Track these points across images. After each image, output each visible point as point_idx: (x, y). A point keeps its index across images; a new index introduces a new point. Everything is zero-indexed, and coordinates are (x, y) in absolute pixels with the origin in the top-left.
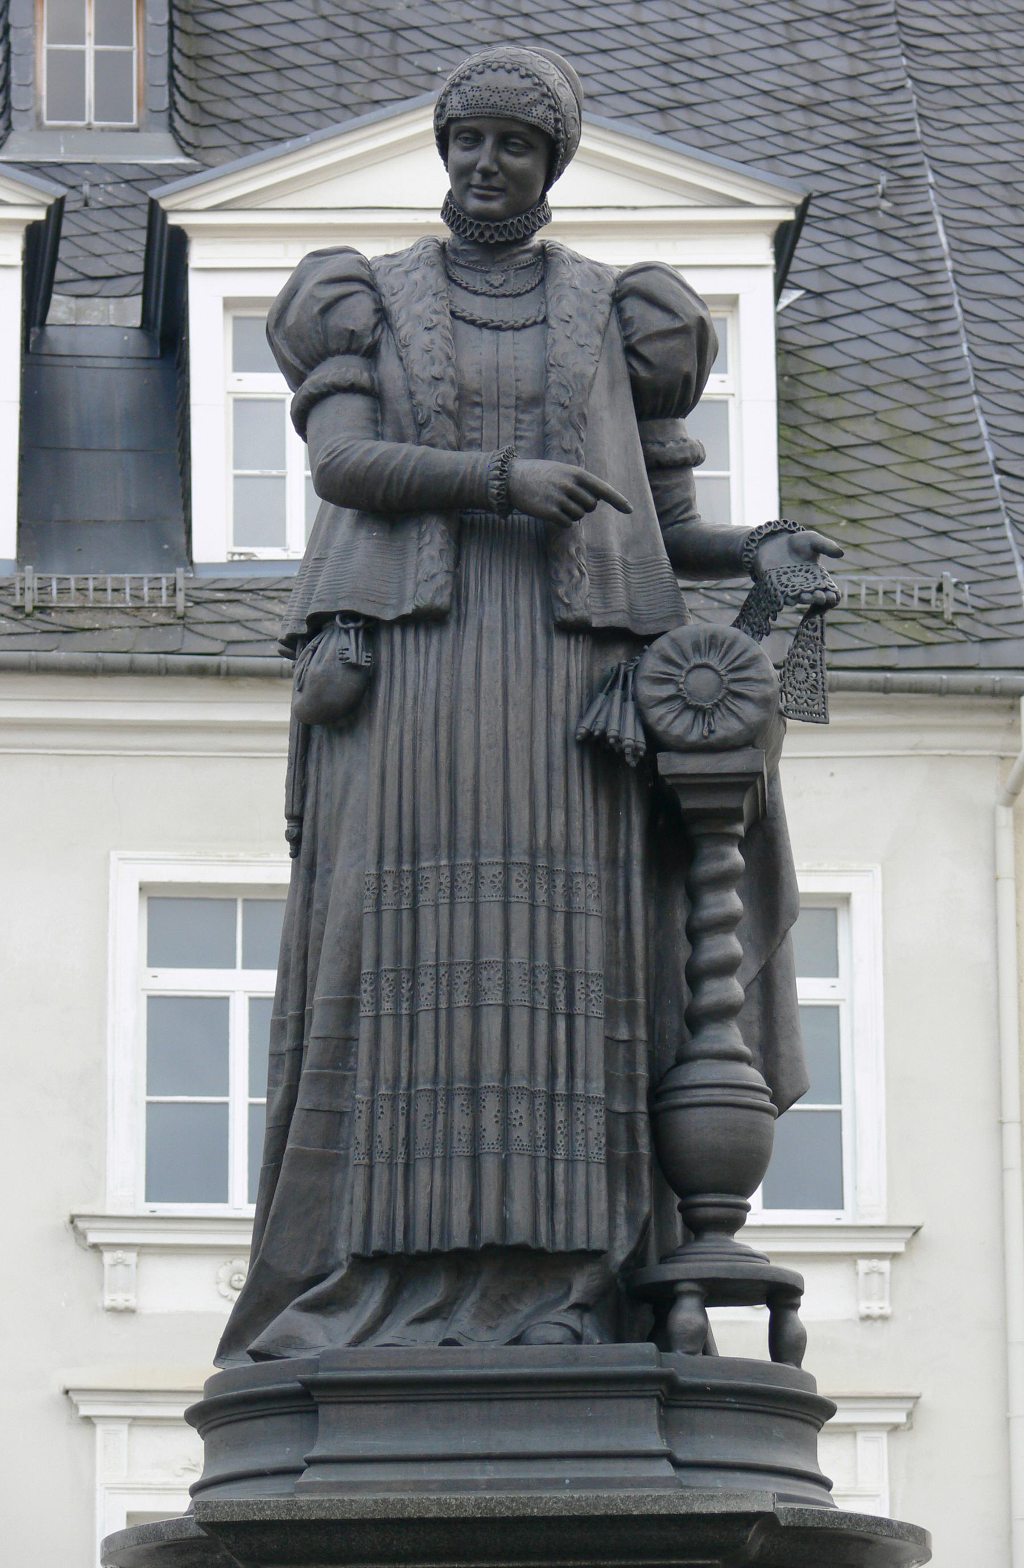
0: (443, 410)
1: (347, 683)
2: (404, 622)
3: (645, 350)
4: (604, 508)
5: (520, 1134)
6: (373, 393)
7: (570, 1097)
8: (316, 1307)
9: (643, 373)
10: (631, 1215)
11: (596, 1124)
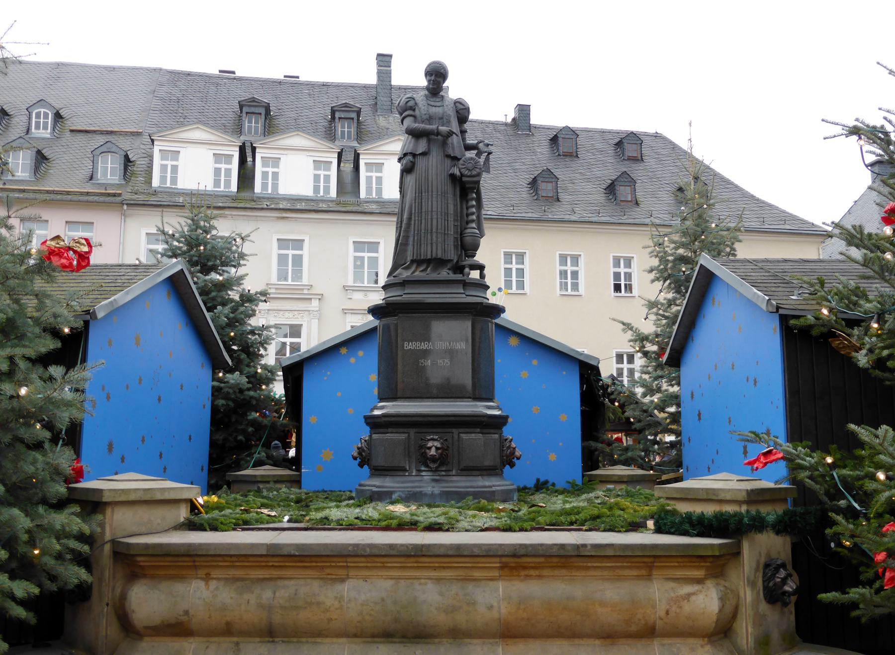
0: (427, 119)
1: (410, 164)
2: (420, 154)
3: (460, 112)
4: (454, 135)
5: (439, 240)
6: (414, 116)
7: (448, 234)
8: (403, 269)
9: (459, 116)
10: (457, 255)
11: (452, 239)
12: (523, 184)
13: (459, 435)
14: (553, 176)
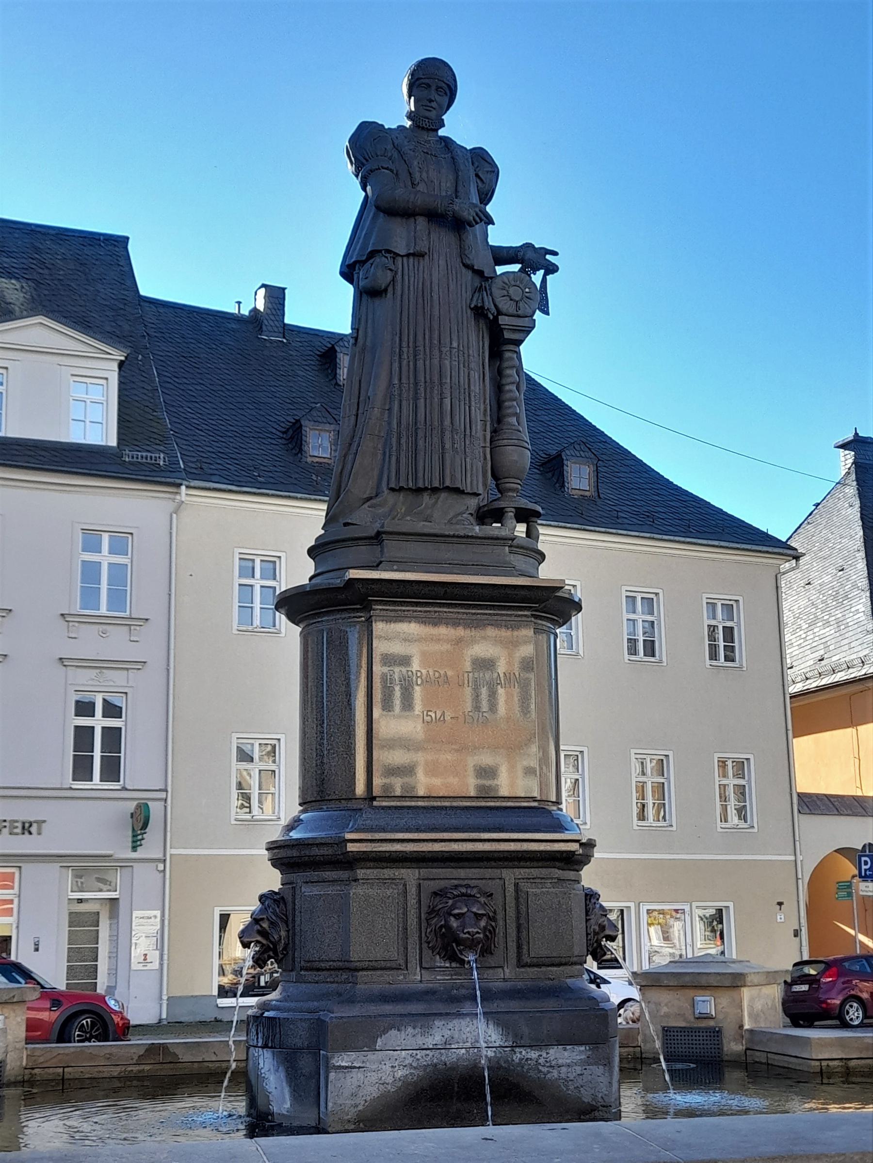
12: (274, 431)
13: (516, 885)
14: (332, 421)
